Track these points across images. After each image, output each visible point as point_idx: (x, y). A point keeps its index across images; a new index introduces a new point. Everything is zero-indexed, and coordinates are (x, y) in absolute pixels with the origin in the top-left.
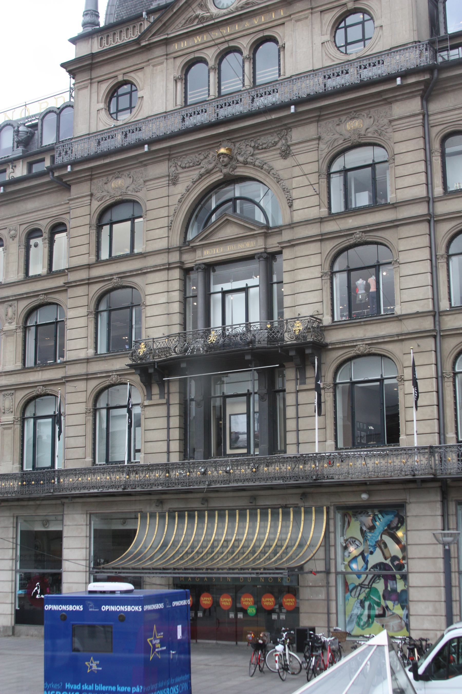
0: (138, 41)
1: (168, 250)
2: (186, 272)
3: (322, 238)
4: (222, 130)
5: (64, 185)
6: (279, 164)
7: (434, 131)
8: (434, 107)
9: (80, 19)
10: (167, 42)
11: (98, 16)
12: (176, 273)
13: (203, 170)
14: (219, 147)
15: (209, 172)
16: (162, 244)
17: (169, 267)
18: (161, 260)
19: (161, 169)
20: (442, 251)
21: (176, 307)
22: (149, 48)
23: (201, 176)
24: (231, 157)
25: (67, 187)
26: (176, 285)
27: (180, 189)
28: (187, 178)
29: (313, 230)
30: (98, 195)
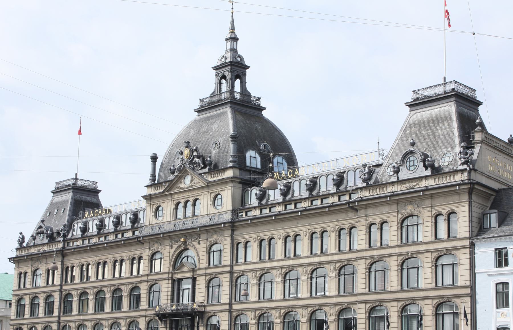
0: (163, 192)
1: (168, 273)
2: (173, 281)
3: (206, 275)
4: (182, 232)
5: (141, 243)
6: (197, 246)
7: (235, 241)
8: (236, 233)
9: (149, 178)
10: (171, 194)
11: (155, 176)
12: (170, 281)
13: (178, 245)
14: (181, 238)
15: (180, 246)
16: (167, 270)
17: (168, 279)
18: (166, 276)
19: (167, 242)
20: (234, 283)
21: (170, 293)
22: (166, 195)
23: (178, 247)
24: (185, 243)
25: (143, 244)
26: (170, 285)
27: (172, 251)
28: (175, 247)
29: (203, 272)
30: (152, 248)
